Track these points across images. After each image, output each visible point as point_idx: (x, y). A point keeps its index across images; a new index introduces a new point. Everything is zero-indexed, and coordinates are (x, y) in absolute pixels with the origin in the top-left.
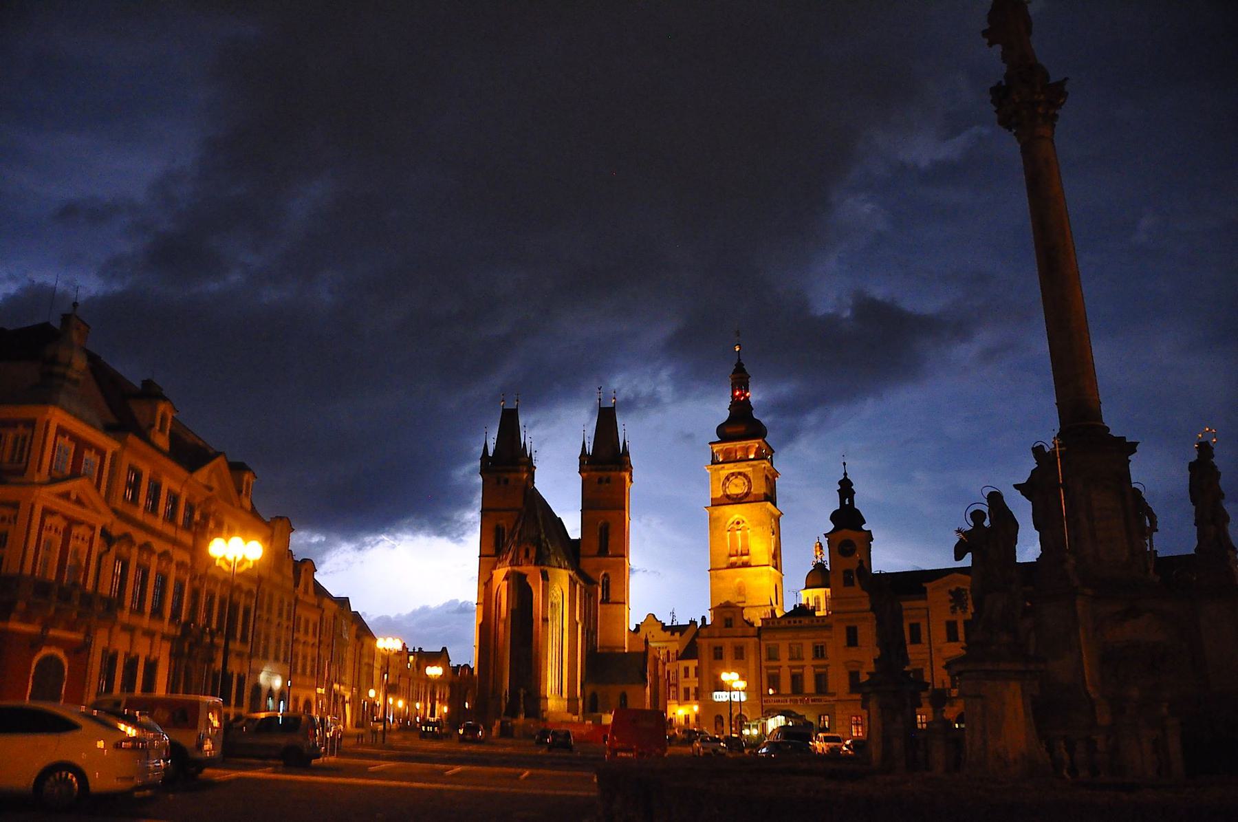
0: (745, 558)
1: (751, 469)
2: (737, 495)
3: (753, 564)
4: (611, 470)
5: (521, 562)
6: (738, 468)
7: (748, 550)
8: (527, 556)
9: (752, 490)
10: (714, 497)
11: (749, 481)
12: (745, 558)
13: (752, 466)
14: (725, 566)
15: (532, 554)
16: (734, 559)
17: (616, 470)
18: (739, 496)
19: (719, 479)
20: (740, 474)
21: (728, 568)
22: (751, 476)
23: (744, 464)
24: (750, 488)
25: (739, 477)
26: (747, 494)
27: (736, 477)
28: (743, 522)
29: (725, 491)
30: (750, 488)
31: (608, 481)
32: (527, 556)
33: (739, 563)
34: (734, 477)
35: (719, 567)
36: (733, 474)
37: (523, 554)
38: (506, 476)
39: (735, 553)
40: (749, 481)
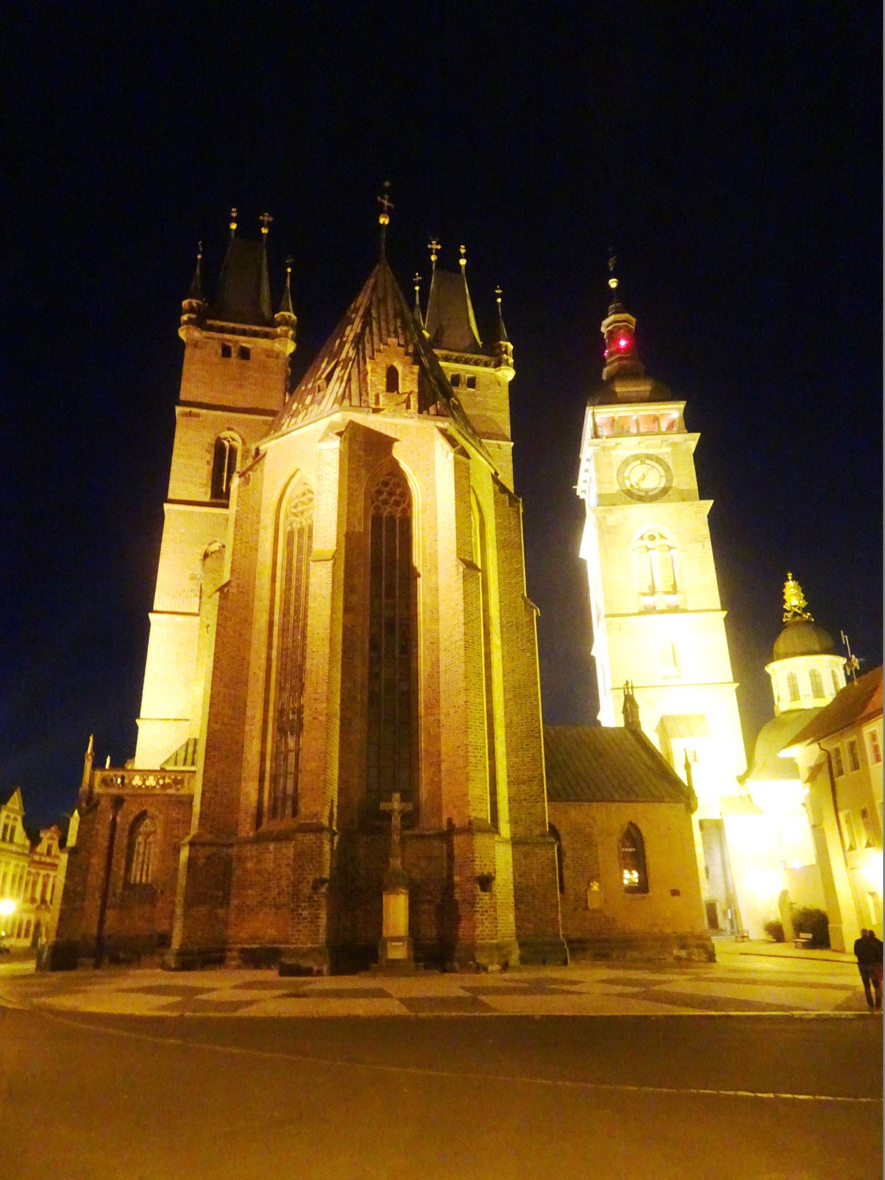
0: (673, 600)
1: (668, 450)
2: (647, 492)
3: (689, 608)
4: (476, 363)
5: (377, 402)
6: (647, 447)
7: (674, 586)
8: (392, 385)
9: (674, 484)
10: (604, 492)
11: (667, 469)
12: (673, 600)
13: (673, 445)
14: (637, 611)
15: (408, 383)
16: (649, 601)
17: (486, 365)
18: (650, 494)
19: (610, 464)
20: (649, 457)
21: (641, 613)
22: (669, 461)
23: (657, 439)
24: (669, 480)
25: (648, 461)
26: (665, 491)
27: (643, 463)
28: (662, 537)
29: (621, 484)
30: (669, 480)
31: (472, 383)
32: (392, 385)
33: (661, 606)
34: (638, 462)
35: (624, 612)
36: (636, 457)
37: (376, 380)
38: (245, 342)
39: (647, 591)
40: (667, 469)
